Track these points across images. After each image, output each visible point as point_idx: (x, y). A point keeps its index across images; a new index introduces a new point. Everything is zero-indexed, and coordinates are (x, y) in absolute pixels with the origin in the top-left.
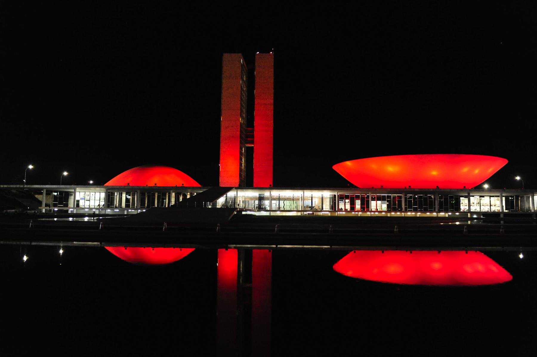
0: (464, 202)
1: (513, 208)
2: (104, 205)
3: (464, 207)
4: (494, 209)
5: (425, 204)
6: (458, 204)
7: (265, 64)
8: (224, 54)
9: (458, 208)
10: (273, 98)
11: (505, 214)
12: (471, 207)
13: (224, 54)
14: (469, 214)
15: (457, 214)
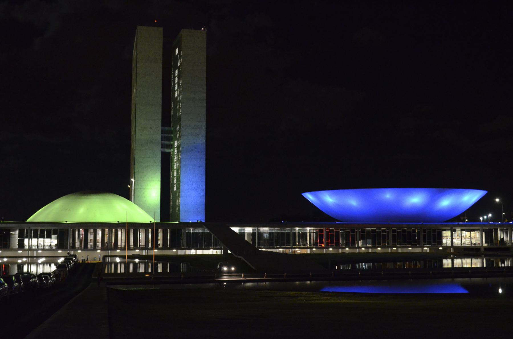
0: (447, 234)
1: (492, 241)
2: (56, 245)
3: (446, 241)
4: (474, 241)
5: (407, 238)
6: (440, 237)
7: (194, 44)
8: (139, 27)
9: (441, 243)
10: (205, 91)
11: (486, 249)
12: (454, 240)
13: (139, 27)
14: (452, 249)
15: (441, 248)
